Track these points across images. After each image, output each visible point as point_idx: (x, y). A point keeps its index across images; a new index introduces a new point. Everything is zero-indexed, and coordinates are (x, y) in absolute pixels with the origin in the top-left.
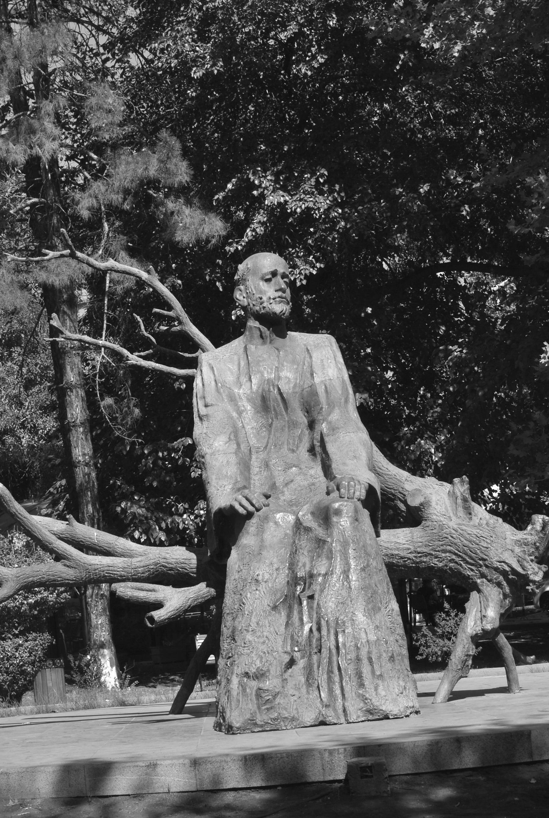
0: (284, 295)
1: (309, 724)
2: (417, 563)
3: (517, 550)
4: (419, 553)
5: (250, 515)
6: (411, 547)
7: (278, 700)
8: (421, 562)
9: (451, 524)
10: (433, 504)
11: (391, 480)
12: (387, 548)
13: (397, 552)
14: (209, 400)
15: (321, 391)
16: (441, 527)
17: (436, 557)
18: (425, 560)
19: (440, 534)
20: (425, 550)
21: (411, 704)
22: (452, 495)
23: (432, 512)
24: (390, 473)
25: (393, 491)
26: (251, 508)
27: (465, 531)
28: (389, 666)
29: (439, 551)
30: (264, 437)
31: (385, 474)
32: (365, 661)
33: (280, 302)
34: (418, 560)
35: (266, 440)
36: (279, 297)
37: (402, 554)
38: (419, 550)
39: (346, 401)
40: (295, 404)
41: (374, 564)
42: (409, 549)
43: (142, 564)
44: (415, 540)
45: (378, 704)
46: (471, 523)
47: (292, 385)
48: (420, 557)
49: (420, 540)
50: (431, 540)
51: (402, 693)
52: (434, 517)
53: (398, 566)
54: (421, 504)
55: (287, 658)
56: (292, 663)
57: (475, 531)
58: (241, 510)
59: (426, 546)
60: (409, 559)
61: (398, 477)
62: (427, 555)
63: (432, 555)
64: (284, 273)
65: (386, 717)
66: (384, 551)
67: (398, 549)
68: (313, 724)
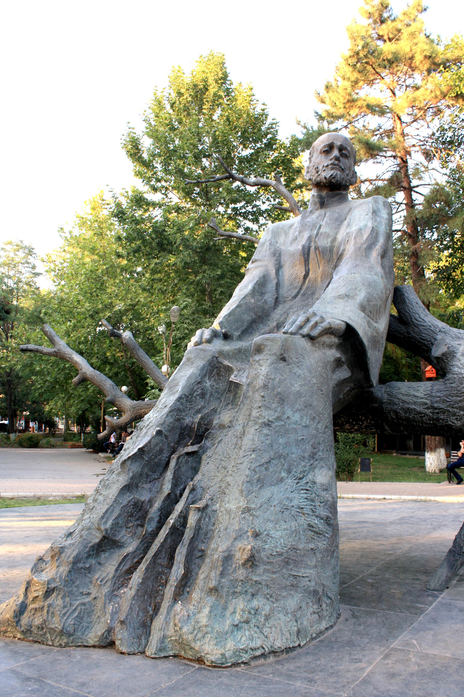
0: (336, 162)
1: (91, 643)
2: (433, 419)
4: (436, 409)
6: (428, 402)
8: (438, 419)
10: (459, 355)
11: (425, 331)
12: (404, 402)
13: (413, 407)
17: (454, 415)
18: (442, 417)
19: (459, 388)
20: (442, 406)
23: (454, 363)
24: (425, 324)
25: (426, 342)
28: (241, 573)
29: (456, 408)
30: (296, 288)
31: (421, 325)
33: (332, 169)
34: (435, 417)
35: (297, 290)
36: (331, 164)
37: (418, 408)
38: (436, 405)
39: (370, 248)
41: (297, 417)
42: (426, 404)
44: (434, 394)
45: (190, 637)
47: (330, 240)
48: (438, 413)
49: (438, 394)
50: (449, 395)
51: (247, 622)
52: (456, 369)
53: (415, 421)
54: (444, 354)
55: (96, 538)
59: (444, 401)
60: (426, 414)
61: (432, 328)
62: (444, 411)
63: (449, 411)
64: (341, 145)
66: (401, 404)
67: (415, 403)
68: (97, 644)
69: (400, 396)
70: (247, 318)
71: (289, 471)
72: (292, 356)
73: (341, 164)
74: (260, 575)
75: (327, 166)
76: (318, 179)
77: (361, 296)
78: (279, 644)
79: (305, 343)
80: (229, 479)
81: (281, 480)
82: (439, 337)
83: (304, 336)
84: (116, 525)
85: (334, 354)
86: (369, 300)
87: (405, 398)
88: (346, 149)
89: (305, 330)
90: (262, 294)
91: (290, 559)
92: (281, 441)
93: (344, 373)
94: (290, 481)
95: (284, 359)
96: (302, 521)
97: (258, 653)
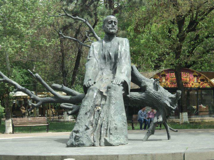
3: (170, 100)
5: (89, 87)
7: (80, 139)
9: (152, 92)
14: (91, 55)
15: (119, 54)
16: (149, 93)
21: (120, 142)
22: (154, 84)
26: (89, 86)
27: (155, 94)
28: (116, 131)
32: (108, 130)
40: (113, 57)
43: (74, 98)
46: (158, 92)
52: (148, 90)
56: (87, 128)
57: (158, 94)
58: (87, 86)
65: (111, 145)
67: (138, 98)
69: (134, 96)
70: (95, 76)
71: (119, 113)
72: (116, 90)
73: (114, 27)
74: (118, 131)
75: (111, 28)
76: (108, 32)
77: (126, 72)
78: (123, 143)
79: (118, 86)
80: (108, 115)
81: (118, 115)
82: (143, 81)
83: (117, 85)
84: (88, 125)
85: (122, 88)
86: (128, 73)
87: (135, 97)
88: (116, 22)
89: (118, 83)
90: (96, 68)
91: (122, 129)
92: (117, 107)
93: (123, 92)
94: (119, 115)
95: (115, 90)
96: (122, 123)
97: (120, 144)
